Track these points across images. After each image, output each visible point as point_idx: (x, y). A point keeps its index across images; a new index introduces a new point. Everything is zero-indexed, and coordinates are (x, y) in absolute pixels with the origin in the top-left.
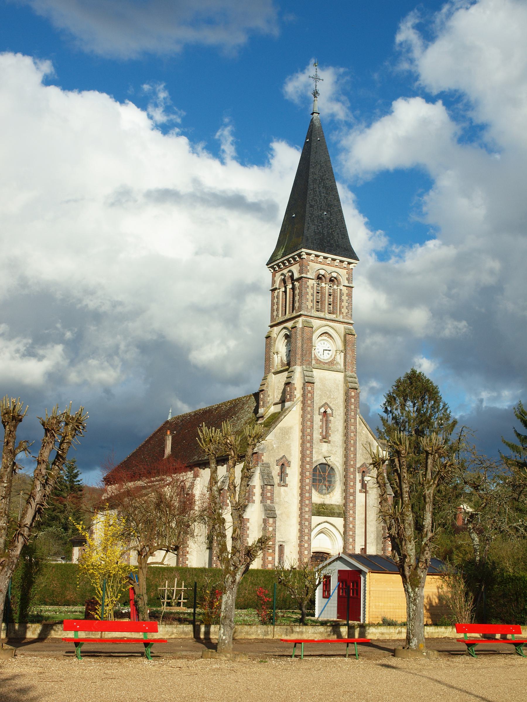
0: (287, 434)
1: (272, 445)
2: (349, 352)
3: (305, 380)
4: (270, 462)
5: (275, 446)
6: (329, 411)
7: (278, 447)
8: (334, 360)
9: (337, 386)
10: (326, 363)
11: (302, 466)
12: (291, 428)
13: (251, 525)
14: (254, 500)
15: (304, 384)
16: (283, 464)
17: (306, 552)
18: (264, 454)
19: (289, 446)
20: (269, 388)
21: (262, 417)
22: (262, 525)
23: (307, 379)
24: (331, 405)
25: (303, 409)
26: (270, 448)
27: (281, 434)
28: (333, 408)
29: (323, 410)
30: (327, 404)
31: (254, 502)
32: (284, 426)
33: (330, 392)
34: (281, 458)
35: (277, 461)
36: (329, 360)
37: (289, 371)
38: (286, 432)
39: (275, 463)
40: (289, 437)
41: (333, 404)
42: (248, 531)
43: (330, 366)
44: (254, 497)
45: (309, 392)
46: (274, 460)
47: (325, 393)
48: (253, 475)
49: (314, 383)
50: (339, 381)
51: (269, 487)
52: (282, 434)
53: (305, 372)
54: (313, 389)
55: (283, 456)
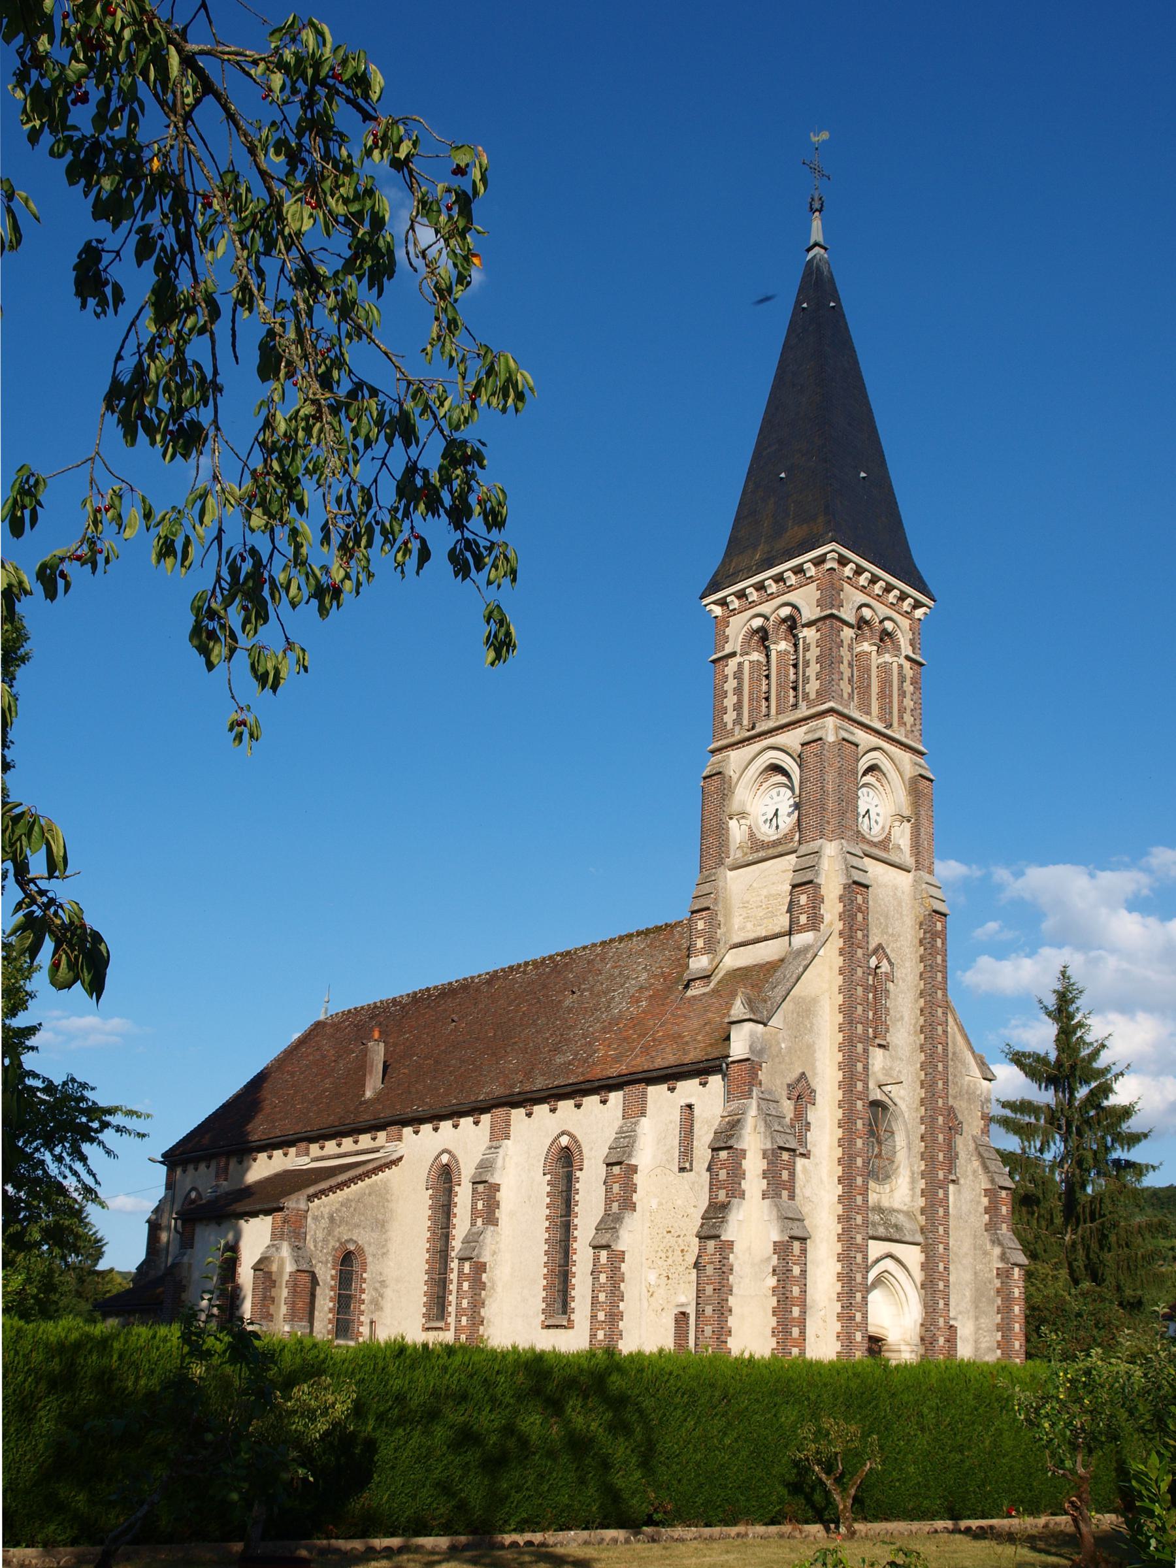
0: (808, 1017)
1: (779, 1043)
2: (924, 821)
3: (849, 876)
4: (774, 1089)
5: (783, 1046)
6: (885, 967)
7: (789, 1048)
8: (888, 839)
9: (900, 904)
10: (874, 845)
11: (847, 1105)
12: (815, 1000)
13: (736, 1258)
14: (744, 1191)
15: (846, 887)
16: (799, 1097)
17: (858, 1336)
18: (764, 1065)
19: (810, 1048)
20: (720, 905)
21: (707, 977)
22: (769, 1258)
23: (857, 876)
24: (888, 951)
25: (848, 952)
26: (774, 1051)
27: (795, 1015)
28: (893, 961)
29: (873, 962)
30: (883, 948)
31: (742, 1195)
32: (803, 994)
33: (887, 917)
34: (799, 1080)
35: (789, 1086)
36: (880, 838)
37: (800, 853)
38: (807, 1010)
39: (785, 1093)
40: (812, 1024)
41: (893, 950)
42: (731, 1277)
43: (880, 851)
44: (743, 1182)
45: (859, 910)
46: (782, 1083)
47: (878, 919)
48: (739, 1121)
49: (867, 887)
50: (903, 893)
51: (785, 1156)
52: (798, 1015)
53: (848, 855)
54: (865, 901)
55: (803, 1073)
